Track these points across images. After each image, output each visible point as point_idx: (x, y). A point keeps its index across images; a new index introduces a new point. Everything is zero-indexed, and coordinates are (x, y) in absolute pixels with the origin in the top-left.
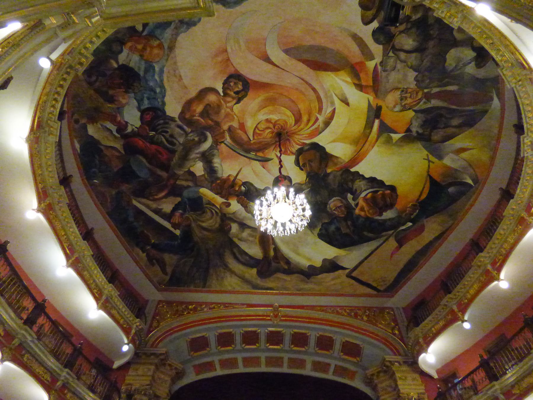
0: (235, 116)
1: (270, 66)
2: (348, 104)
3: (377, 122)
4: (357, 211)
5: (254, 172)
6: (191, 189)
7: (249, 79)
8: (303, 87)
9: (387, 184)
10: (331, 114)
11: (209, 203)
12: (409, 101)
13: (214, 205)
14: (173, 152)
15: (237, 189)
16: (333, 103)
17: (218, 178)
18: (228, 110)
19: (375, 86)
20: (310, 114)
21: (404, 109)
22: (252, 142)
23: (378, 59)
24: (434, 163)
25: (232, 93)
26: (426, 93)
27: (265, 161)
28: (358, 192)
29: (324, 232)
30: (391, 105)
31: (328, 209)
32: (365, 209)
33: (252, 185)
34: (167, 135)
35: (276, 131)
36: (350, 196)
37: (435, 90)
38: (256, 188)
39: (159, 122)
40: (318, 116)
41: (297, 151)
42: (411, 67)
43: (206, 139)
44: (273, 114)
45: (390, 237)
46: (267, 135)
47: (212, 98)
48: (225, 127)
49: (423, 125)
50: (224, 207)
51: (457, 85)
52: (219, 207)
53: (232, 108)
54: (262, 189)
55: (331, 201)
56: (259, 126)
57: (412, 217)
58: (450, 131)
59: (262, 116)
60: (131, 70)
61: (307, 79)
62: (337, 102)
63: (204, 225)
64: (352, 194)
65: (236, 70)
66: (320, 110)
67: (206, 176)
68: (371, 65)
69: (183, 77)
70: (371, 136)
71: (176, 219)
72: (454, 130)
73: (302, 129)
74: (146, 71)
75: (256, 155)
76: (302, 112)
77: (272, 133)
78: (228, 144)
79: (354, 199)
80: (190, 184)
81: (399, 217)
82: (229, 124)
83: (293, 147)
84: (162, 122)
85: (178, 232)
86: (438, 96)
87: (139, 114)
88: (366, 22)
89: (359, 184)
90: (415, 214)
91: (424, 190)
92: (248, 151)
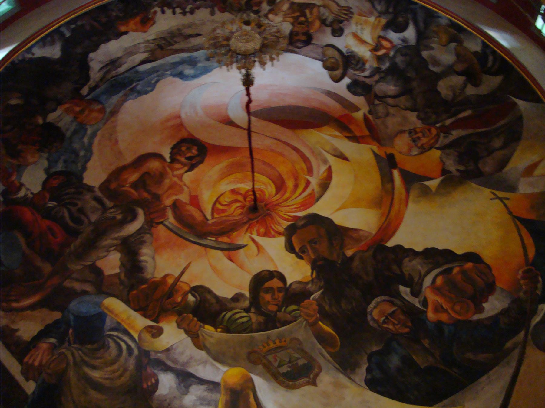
0: (185, 188)
1: (234, 129)
2: (346, 159)
3: (396, 174)
4: (431, 315)
5: (214, 269)
6: (87, 298)
7: (206, 143)
8: (280, 148)
9: (460, 252)
10: (326, 174)
11: (118, 328)
12: (424, 140)
13: (126, 332)
14: (75, 234)
15: (179, 299)
16: (325, 161)
17: (144, 281)
18: (175, 179)
19: (372, 133)
20: (296, 179)
21: (423, 150)
22: (210, 222)
23: (364, 109)
24: (508, 199)
25: (183, 160)
26: (440, 127)
27: (231, 249)
28: (416, 279)
29: (377, 374)
30: (405, 149)
31: (371, 323)
32: (444, 306)
33: (209, 291)
34: (74, 209)
35: (248, 204)
36: (404, 291)
37: (448, 122)
38: (216, 297)
39: (67, 191)
40: (308, 177)
41: (285, 229)
42: (406, 109)
43: (134, 217)
44: (241, 183)
45: (524, 347)
46: (235, 212)
47: (154, 165)
48: (168, 202)
49: (460, 160)
50: (147, 336)
51: (470, 108)
52: (136, 336)
53: (180, 177)
54: (230, 296)
55: (371, 306)
56: (221, 199)
57: (539, 292)
58: (499, 155)
59: (225, 186)
60: (58, 129)
61: (284, 138)
62: (331, 160)
63: (96, 375)
64: (406, 286)
65: (190, 134)
66: (310, 171)
67: (123, 276)
68: (359, 115)
69: (120, 142)
70: (396, 192)
71: (39, 356)
72: (503, 152)
73: (288, 199)
74: (75, 132)
75: (216, 241)
76: (285, 177)
77: (242, 207)
78: (171, 226)
79: (415, 293)
80: (88, 288)
81: (516, 301)
82: (175, 197)
83: (279, 224)
84: (73, 190)
85: (30, 387)
86: (455, 125)
87: (44, 176)
88: (337, 80)
89: (412, 266)
90: (540, 286)
91: (526, 242)
92: (203, 235)
